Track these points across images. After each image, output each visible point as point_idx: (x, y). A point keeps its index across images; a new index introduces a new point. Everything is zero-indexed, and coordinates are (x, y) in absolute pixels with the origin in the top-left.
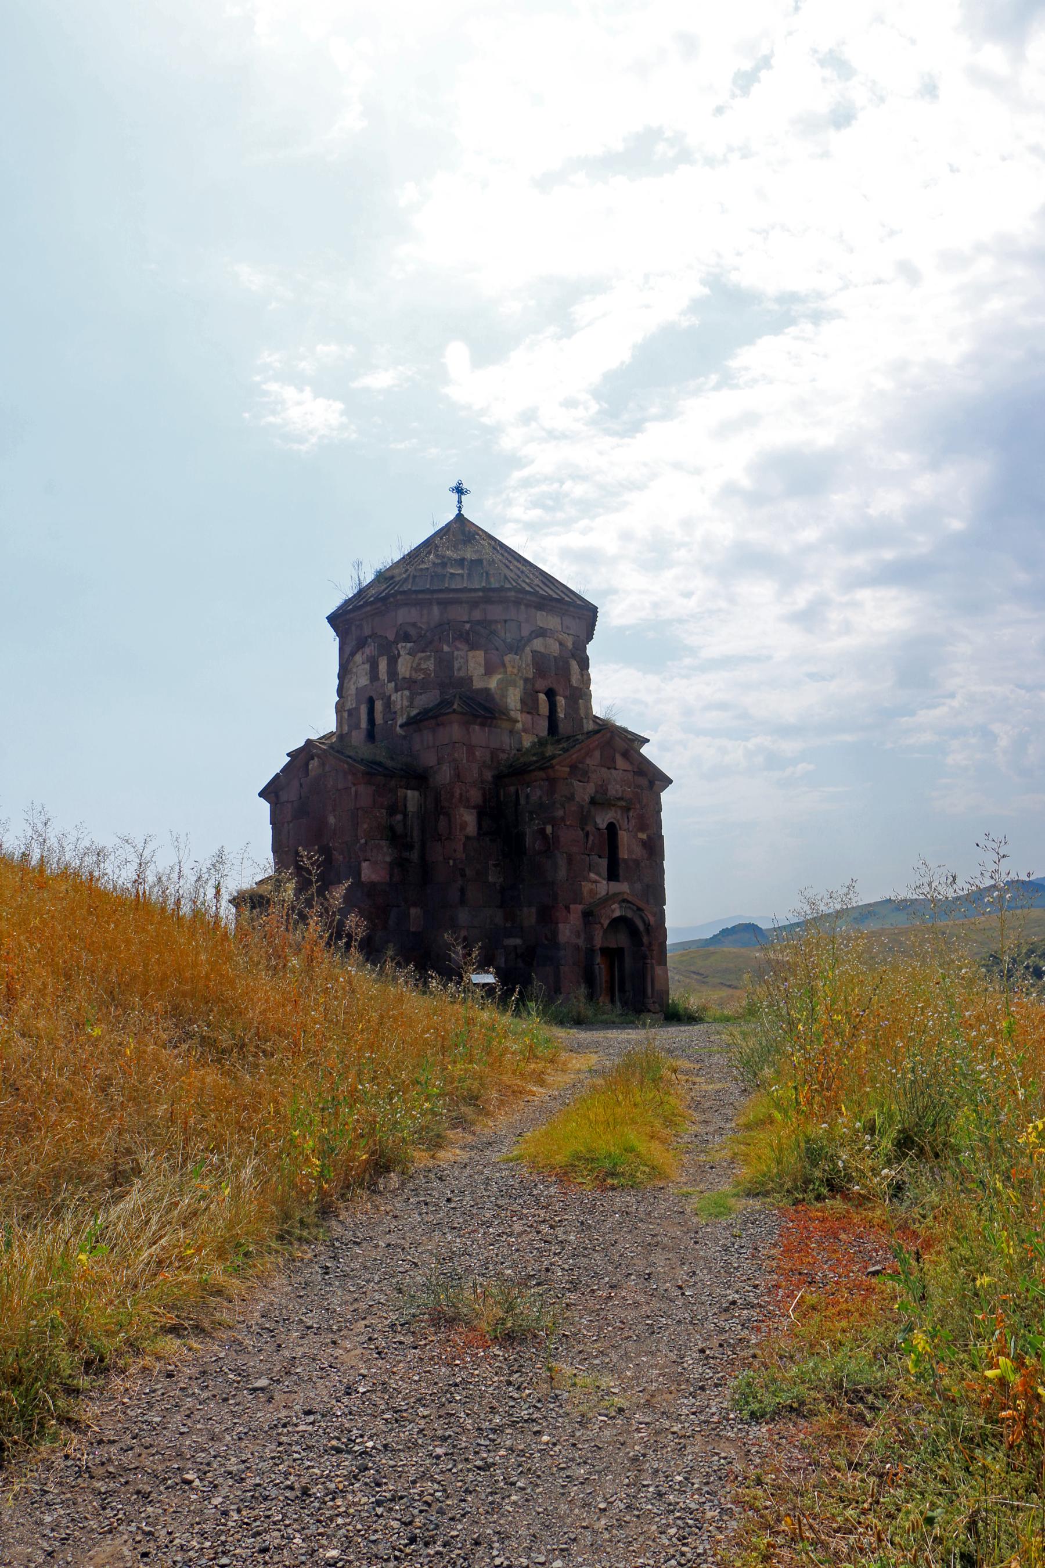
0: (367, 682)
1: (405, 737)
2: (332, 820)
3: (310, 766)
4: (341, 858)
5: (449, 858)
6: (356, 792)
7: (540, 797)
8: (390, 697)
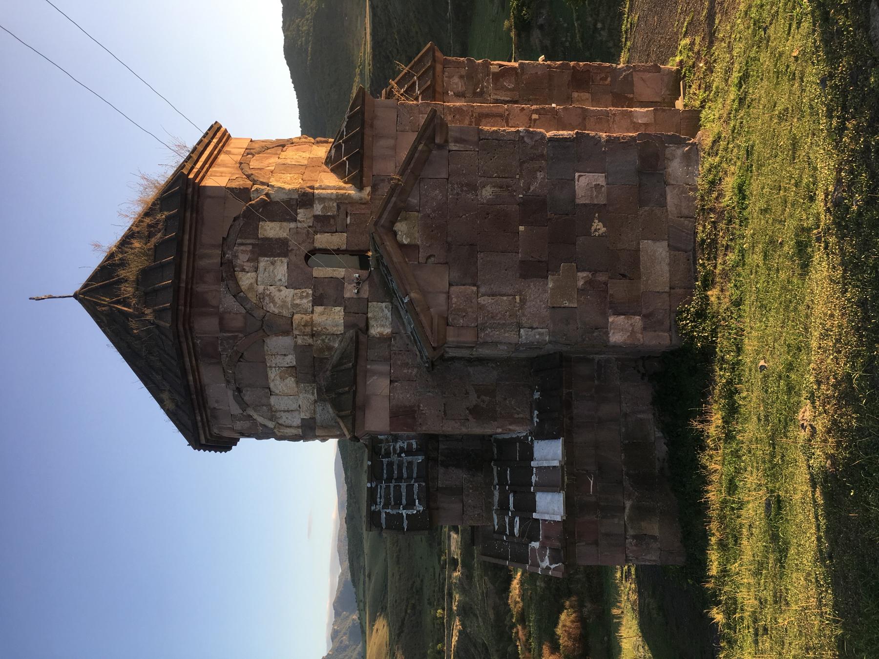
0: (285, 260)
1: (374, 188)
2: (487, 193)
3: (405, 242)
4: (540, 176)
5: (530, 119)
6: (457, 141)
7: (461, 77)
8: (316, 217)
